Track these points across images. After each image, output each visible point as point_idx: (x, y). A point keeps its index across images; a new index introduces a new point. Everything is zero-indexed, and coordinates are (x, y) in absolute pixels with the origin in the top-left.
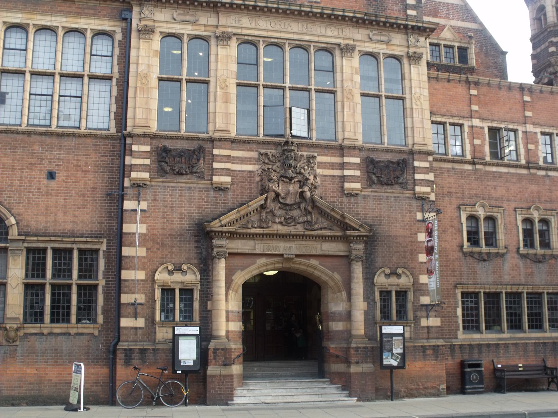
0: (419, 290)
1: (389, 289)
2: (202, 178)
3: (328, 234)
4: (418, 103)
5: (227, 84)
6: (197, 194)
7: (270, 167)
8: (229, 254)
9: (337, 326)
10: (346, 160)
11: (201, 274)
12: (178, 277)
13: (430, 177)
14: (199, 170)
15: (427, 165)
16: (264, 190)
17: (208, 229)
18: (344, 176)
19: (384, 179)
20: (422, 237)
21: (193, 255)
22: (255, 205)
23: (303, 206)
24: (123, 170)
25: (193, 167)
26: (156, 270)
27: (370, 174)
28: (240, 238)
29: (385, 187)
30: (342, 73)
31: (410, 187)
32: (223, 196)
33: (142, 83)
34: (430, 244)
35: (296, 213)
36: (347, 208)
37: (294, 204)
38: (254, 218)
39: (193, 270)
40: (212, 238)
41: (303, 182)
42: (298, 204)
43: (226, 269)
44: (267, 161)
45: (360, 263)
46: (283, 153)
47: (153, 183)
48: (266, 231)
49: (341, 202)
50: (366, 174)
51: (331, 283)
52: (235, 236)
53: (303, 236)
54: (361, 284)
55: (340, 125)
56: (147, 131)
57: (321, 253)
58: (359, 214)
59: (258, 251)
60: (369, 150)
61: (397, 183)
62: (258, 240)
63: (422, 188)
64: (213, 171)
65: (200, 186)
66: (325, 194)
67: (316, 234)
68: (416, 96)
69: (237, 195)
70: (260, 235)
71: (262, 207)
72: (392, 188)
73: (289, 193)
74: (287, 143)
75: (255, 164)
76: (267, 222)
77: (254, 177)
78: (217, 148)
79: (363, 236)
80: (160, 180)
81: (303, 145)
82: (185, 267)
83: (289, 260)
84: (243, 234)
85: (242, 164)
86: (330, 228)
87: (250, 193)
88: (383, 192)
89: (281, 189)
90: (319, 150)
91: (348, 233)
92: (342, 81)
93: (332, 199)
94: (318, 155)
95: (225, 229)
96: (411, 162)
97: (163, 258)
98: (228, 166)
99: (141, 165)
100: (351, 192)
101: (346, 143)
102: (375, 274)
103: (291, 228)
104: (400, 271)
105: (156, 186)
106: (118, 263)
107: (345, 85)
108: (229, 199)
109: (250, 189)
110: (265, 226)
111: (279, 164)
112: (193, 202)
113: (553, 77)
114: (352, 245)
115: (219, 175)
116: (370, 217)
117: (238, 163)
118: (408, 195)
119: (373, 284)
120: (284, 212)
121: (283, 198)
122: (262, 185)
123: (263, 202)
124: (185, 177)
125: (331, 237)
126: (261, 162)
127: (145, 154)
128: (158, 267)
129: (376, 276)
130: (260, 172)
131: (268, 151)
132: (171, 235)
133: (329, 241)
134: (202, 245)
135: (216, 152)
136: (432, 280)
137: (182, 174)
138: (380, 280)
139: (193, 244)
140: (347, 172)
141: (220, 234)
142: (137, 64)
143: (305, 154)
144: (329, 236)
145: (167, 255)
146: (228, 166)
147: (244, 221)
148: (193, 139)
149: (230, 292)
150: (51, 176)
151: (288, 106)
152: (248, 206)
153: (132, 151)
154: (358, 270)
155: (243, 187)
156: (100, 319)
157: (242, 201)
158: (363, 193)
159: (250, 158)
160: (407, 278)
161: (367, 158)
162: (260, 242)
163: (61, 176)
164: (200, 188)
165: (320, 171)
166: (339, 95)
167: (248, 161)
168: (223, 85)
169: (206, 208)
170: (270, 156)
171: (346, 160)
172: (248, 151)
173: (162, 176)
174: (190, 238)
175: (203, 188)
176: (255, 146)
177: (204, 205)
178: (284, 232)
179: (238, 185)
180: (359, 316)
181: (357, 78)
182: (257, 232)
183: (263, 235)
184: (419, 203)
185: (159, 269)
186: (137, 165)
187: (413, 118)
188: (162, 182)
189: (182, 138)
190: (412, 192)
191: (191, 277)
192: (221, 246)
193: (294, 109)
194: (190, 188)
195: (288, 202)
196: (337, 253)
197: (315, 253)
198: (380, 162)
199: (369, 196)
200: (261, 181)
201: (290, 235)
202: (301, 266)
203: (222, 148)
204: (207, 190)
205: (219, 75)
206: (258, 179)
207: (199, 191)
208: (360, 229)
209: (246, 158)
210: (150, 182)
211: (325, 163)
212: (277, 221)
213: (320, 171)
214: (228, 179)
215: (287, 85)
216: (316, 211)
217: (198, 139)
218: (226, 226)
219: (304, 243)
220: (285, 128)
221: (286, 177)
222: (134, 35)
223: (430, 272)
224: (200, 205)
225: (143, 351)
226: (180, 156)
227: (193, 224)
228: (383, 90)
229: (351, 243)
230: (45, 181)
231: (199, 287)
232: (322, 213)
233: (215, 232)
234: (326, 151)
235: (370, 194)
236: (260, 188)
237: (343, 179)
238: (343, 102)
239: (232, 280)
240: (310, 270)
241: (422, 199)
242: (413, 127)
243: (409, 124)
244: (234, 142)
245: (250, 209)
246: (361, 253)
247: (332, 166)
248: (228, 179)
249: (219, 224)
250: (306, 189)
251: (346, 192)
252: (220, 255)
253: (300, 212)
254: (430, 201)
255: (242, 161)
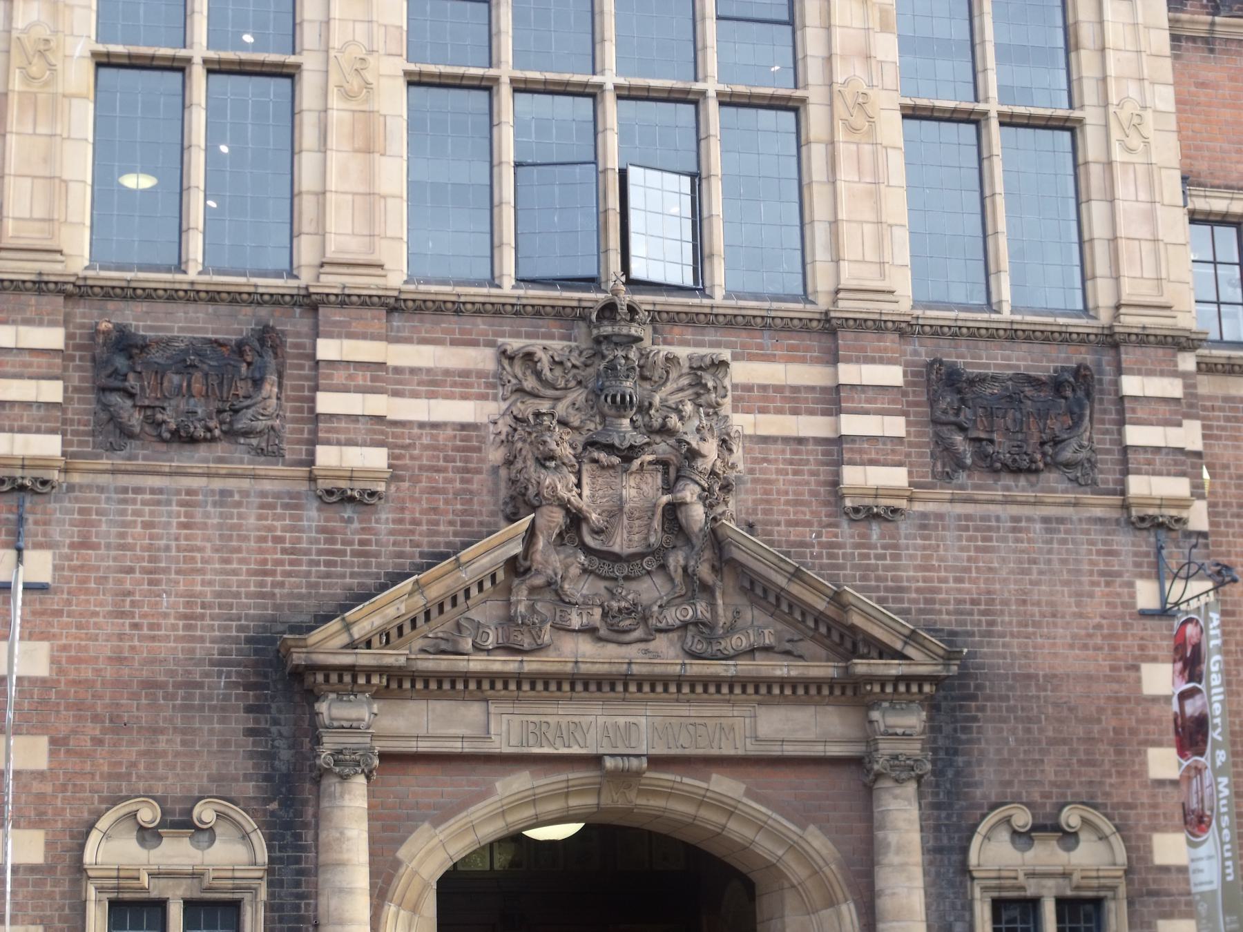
0: (1151, 893)
1: (1030, 892)
2: (271, 453)
3: (778, 673)
4: (1135, 142)
5: (369, 77)
6: (252, 521)
7: (544, 407)
8: (385, 757)
10: (849, 373)
11: (270, 839)
12: (177, 852)
13: (1189, 435)
14: (261, 424)
15: (1172, 388)
16: (520, 502)
17: (298, 658)
18: (840, 440)
19: (1002, 447)
20: (1160, 679)
21: (238, 764)
22: (485, 561)
23: (676, 560)
25: (236, 411)
26: (91, 826)
27: (944, 430)
28: (427, 695)
29: (1007, 480)
30: (828, 28)
31: (1107, 477)
32: (356, 525)
33: (29, 78)
34: (1191, 708)
35: (649, 590)
36: (854, 567)
37: (642, 556)
38: (485, 611)
39: (237, 824)
40: (313, 696)
41: (680, 465)
42: (658, 554)
43: (372, 818)
44: (530, 383)
45: (911, 788)
46: (598, 351)
47: (76, 478)
48: (532, 665)
49: (831, 545)
50: (930, 430)
51: (796, 871)
52: (407, 685)
53: (679, 681)
54: (918, 872)
55: (820, 234)
56: (51, 268)
57: (752, 749)
58: (901, 589)
59: (499, 745)
60: (937, 332)
61: (1054, 464)
62: (498, 699)
63: (1155, 480)
64: (316, 428)
65: (267, 486)
66: (765, 512)
67: (732, 672)
68: (1124, 115)
69: (415, 522)
70: (505, 678)
71: (516, 568)
72: (1032, 485)
73: (621, 509)
74: (609, 310)
75: (483, 397)
76: (533, 629)
77: (479, 450)
78: (330, 335)
79: (921, 679)
80: (105, 463)
81: (674, 318)
82: (205, 813)
83: (625, 778)
84: (440, 677)
85: (431, 396)
86: (788, 646)
87: (464, 512)
88: (998, 500)
89: (590, 496)
90: (741, 337)
91: (861, 667)
92: (829, 59)
93: (795, 534)
94: (735, 357)
95: (364, 658)
96: (1107, 378)
97: (119, 776)
98: (377, 404)
99: (27, 405)
100: (868, 501)
101: (849, 306)
102: (973, 829)
103: (633, 652)
104: (1071, 817)
105: (89, 487)
107: (839, 78)
108: (384, 538)
109: (466, 495)
110: (527, 642)
111: (579, 395)
112: (239, 550)
114: (875, 715)
115: (339, 443)
116: (947, 602)
117: (415, 395)
118: (1098, 512)
119: (964, 870)
120: (602, 585)
121: (597, 532)
122: (514, 482)
123: (517, 548)
124: (203, 450)
125: (794, 683)
126: (509, 388)
127: (43, 360)
128: (99, 815)
129: (976, 841)
130: (505, 430)
131: (536, 345)
132: (150, 685)
133: (783, 701)
134: (276, 722)
135: (327, 349)
136: (1203, 851)
137: (193, 440)
138: (993, 853)
139: (239, 721)
140: (851, 425)
141: (348, 679)
143: (682, 352)
144: (783, 682)
145: (134, 765)
146: (377, 404)
147: (441, 626)
148: (235, 298)
149: (390, 910)
151: (613, 163)
152: (459, 565)
154: (903, 818)
155: (437, 491)
157: (431, 544)
158: (918, 507)
159: (465, 373)
160: (1101, 847)
161: (930, 365)
162: (508, 707)
164: (263, 494)
165: (743, 423)
166: (815, 116)
167: (454, 384)
168: (355, 83)
169: (289, 574)
170: (545, 365)
171: (849, 373)
172: (454, 343)
173: (112, 448)
174: (226, 698)
175: (277, 495)
176: (481, 325)
177: (279, 562)
178: (604, 669)
179: (415, 480)
181: (887, 47)
182: (497, 667)
183: (519, 678)
184: (1146, 542)
185: (103, 824)
186: (13, 403)
187: (1112, 201)
188: (114, 472)
189: (192, 296)
190: (1117, 499)
191: (232, 854)
192: (352, 728)
193: (634, 174)
194: (224, 493)
195: (616, 549)
196: (818, 750)
197: (728, 750)
198: (982, 379)
199: (940, 516)
200: (509, 463)
201: (626, 679)
202: (673, 802)
203: (351, 336)
204: (293, 503)
205: (336, 42)
206: (495, 455)
207: (262, 506)
208: (910, 651)
209: (447, 372)
210: (65, 471)
211: (764, 388)
212: (576, 621)
213: (743, 423)
214: (375, 458)
215: (610, 78)
216: (730, 582)
217: (257, 299)
218: (368, 644)
219: (684, 710)
220: (602, 251)
221: (610, 448)
223: (1196, 822)
224: (265, 562)
226: (186, 368)
227: (236, 640)
228: (993, 93)
229: (870, 707)
231: (263, 894)
232: (756, 589)
233: (327, 669)
234: (766, 339)
235: (946, 508)
236: (503, 493)
237: (837, 449)
238: (832, 143)
239: (397, 864)
240: (711, 818)
241: (1157, 525)
242: (1114, 239)
243: (1098, 226)
244: (395, 309)
245: (466, 576)
246: (914, 748)
247: (792, 399)
248: (375, 458)
249: (344, 639)
250: (689, 493)
251: (848, 503)
252: (345, 764)
253: (668, 587)
254: (1189, 534)
255: (434, 383)
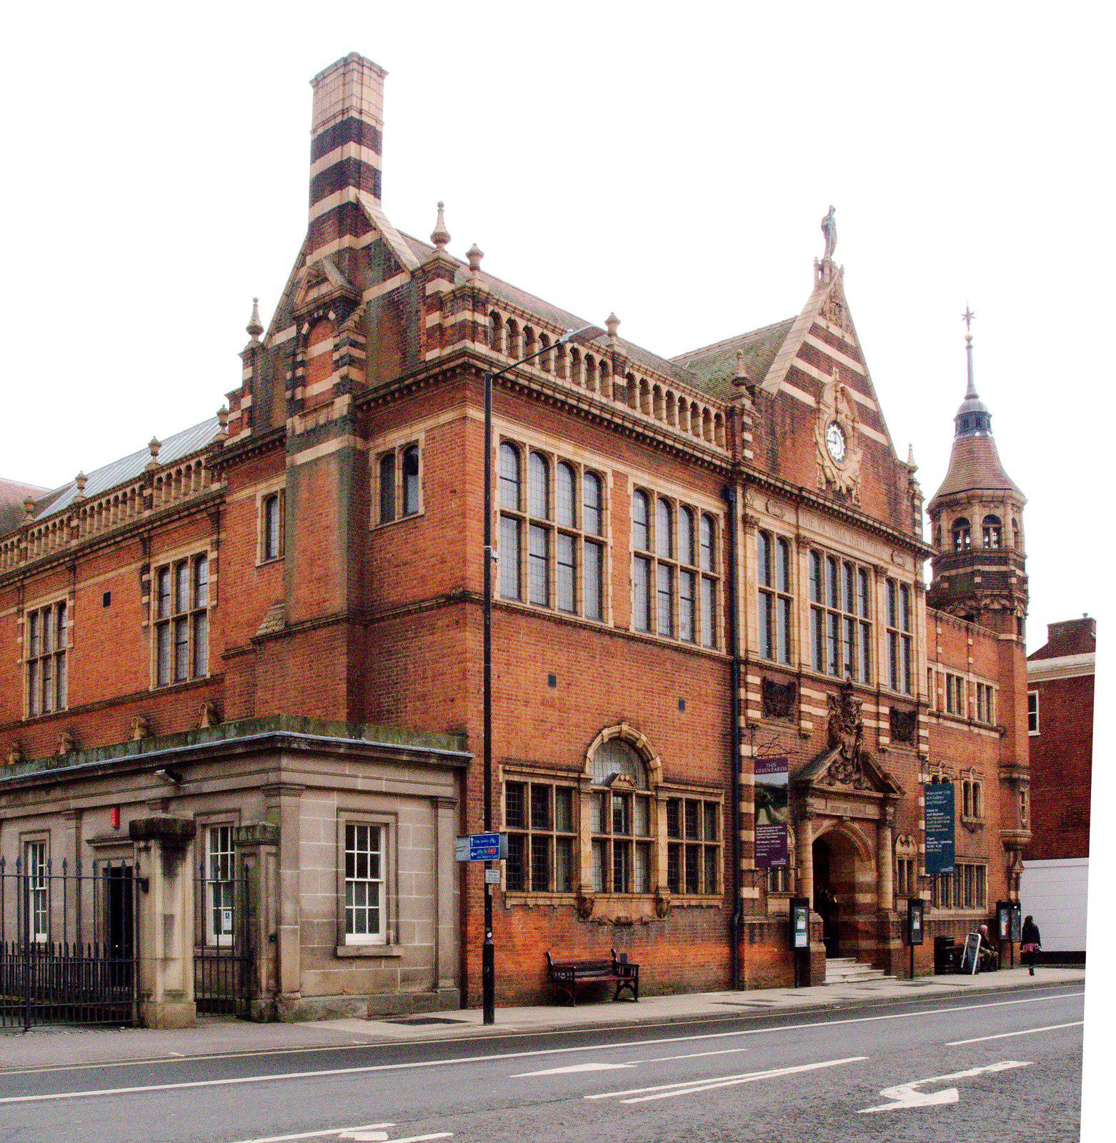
9: (865, 898)
24: (735, 707)
40: (805, 795)
51: (862, 850)
88: (901, 745)
104: (910, 838)
106: (737, 822)
113: (975, 612)
142: (745, 567)
150: (682, 705)
153: (746, 683)
156: (722, 888)
163: (689, 705)
180: (889, 886)
222: (740, 526)
225: (761, 925)
230: (677, 712)
